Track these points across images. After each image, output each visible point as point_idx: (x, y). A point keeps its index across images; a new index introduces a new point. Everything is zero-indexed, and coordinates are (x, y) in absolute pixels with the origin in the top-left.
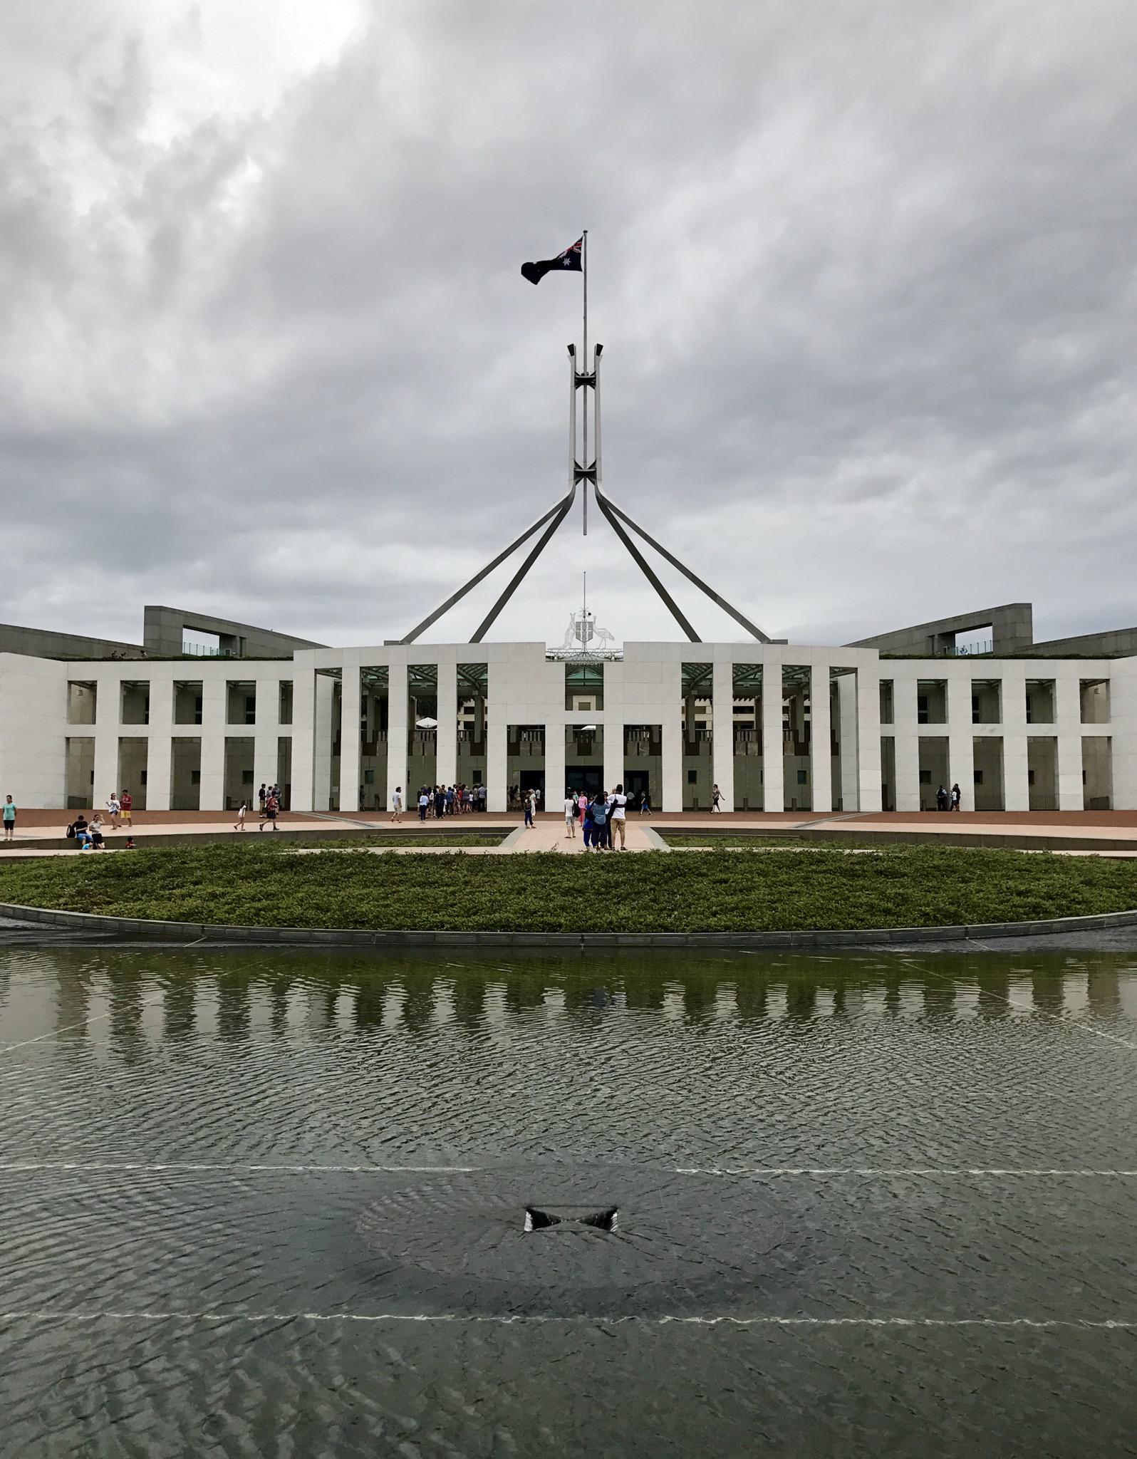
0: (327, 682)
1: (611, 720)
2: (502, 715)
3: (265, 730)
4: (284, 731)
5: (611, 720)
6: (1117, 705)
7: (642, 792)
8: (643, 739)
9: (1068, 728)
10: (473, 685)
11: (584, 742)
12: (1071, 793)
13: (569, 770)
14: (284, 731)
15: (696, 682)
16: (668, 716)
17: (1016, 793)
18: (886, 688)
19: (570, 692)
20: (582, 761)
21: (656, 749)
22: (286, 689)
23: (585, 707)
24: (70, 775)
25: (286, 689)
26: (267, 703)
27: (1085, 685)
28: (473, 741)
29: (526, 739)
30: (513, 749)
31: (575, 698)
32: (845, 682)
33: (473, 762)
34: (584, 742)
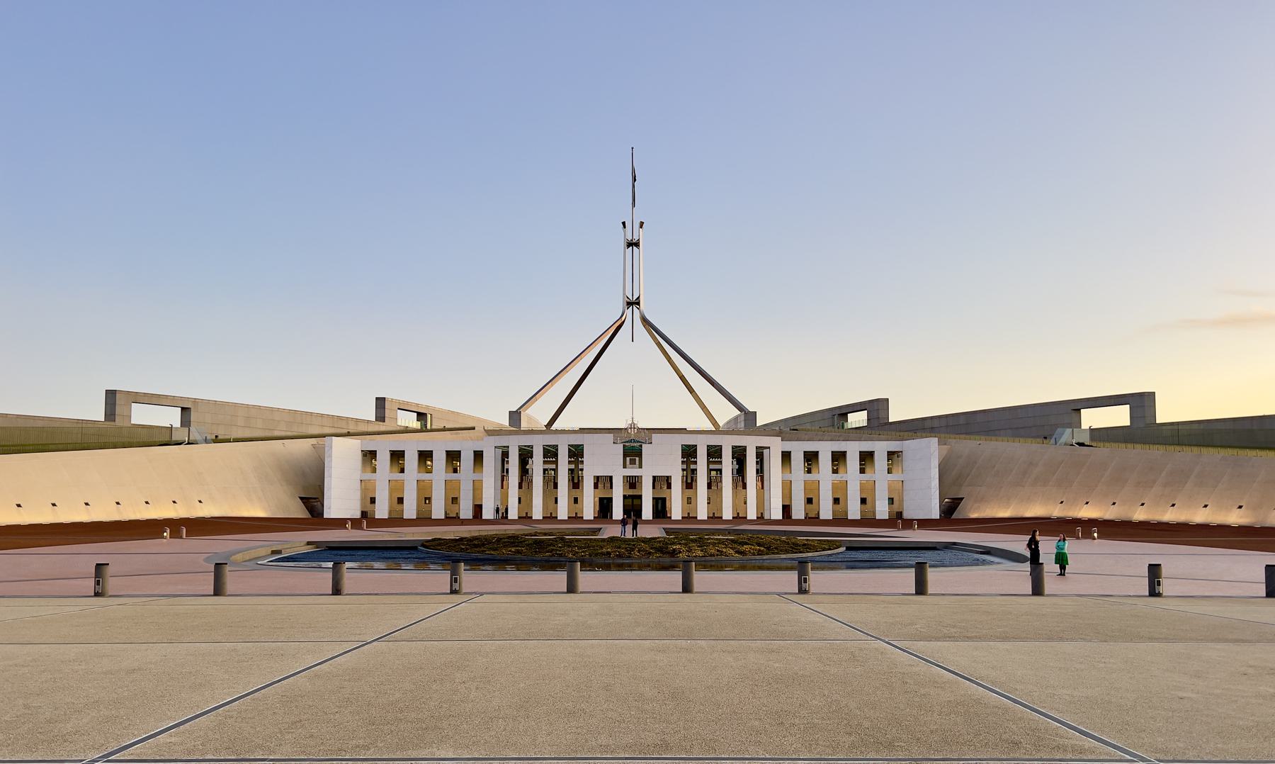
1: (646, 474)
4: (476, 477)
8: (662, 482)
10: (576, 453)
11: (633, 483)
13: (625, 497)
14: (476, 477)
15: (689, 453)
18: (786, 456)
19: (625, 456)
20: (631, 492)
21: (669, 486)
22: (478, 456)
23: (632, 462)
24: (363, 499)
25: (478, 456)
27: (891, 455)
28: (576, 483)
29: (603, 482)
30: (596, 486)
32: (766, 451)
33: (576, 493)
34: (633, 483)
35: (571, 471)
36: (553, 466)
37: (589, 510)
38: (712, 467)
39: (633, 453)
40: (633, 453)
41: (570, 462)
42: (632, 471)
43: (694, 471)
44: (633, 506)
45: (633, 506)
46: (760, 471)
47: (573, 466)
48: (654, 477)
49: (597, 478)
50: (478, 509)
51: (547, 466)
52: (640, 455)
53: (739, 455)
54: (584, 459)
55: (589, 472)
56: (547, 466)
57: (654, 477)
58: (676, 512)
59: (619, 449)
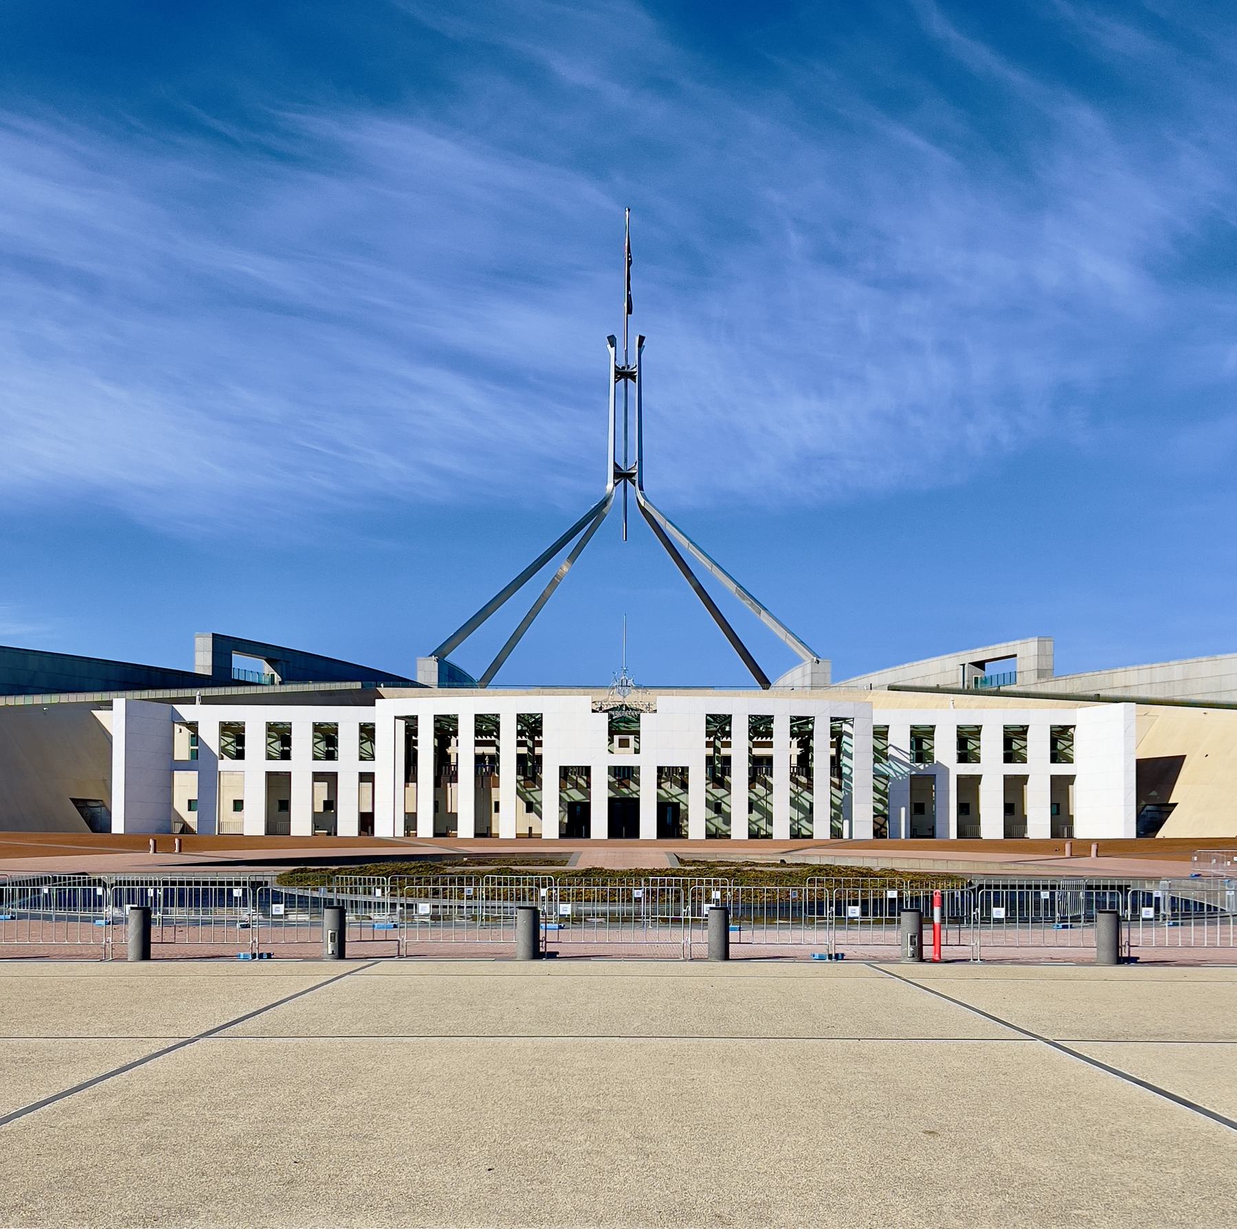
0: (401, 725)
1: (647, 761)
2: (555, 753)
3: (347, 764)
5: (647, 761)
6: (1081, 746)
7: (671, 821)
8: (674, 775)
9: (1039, 769)
10: (531, 727)
11: (624, 775)
12: (1038, 824)
15: (718, 726)
16: (692, 754)
17: (992, 823)
19: (611, 733)
21: (684, 786)
22: (367, 732)
23: (624, 744)
25: (367, 732)
26: (348, 741)
29: (575, 776)
31: (616, 738)
34: (624, 775)
35: (521, 758)
36: (492, 750)
37: (550, 823)
38: (757, 752)
39: (623, 726)
40: (623, 726)
41: (520, 744)
42: (624, 758)
43: (727, 760)
44: (624, 818)
45: (624, 818)
46: (835, 763)
47: (524, 750)
48: (660, 769)
49: (565, 772)
50: (367, 821)
51: (480, 750)
52: (637, 734)
53: (802, 730)
54: (544, 738)
55: (552, 760)
56: (480, 750)
57: (660, 769)
58: (696, 826)
59: (604, 718)
